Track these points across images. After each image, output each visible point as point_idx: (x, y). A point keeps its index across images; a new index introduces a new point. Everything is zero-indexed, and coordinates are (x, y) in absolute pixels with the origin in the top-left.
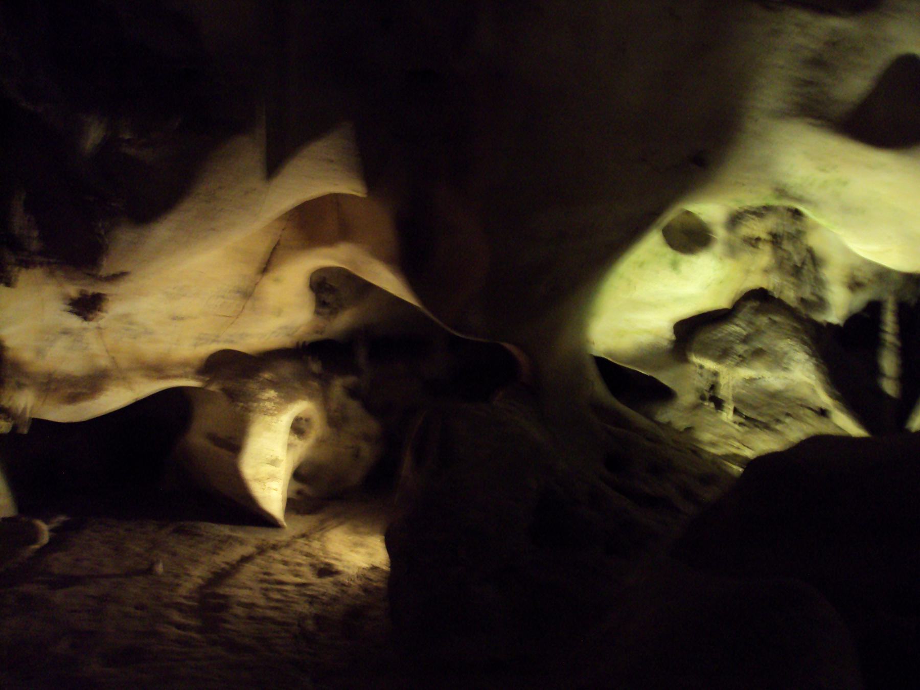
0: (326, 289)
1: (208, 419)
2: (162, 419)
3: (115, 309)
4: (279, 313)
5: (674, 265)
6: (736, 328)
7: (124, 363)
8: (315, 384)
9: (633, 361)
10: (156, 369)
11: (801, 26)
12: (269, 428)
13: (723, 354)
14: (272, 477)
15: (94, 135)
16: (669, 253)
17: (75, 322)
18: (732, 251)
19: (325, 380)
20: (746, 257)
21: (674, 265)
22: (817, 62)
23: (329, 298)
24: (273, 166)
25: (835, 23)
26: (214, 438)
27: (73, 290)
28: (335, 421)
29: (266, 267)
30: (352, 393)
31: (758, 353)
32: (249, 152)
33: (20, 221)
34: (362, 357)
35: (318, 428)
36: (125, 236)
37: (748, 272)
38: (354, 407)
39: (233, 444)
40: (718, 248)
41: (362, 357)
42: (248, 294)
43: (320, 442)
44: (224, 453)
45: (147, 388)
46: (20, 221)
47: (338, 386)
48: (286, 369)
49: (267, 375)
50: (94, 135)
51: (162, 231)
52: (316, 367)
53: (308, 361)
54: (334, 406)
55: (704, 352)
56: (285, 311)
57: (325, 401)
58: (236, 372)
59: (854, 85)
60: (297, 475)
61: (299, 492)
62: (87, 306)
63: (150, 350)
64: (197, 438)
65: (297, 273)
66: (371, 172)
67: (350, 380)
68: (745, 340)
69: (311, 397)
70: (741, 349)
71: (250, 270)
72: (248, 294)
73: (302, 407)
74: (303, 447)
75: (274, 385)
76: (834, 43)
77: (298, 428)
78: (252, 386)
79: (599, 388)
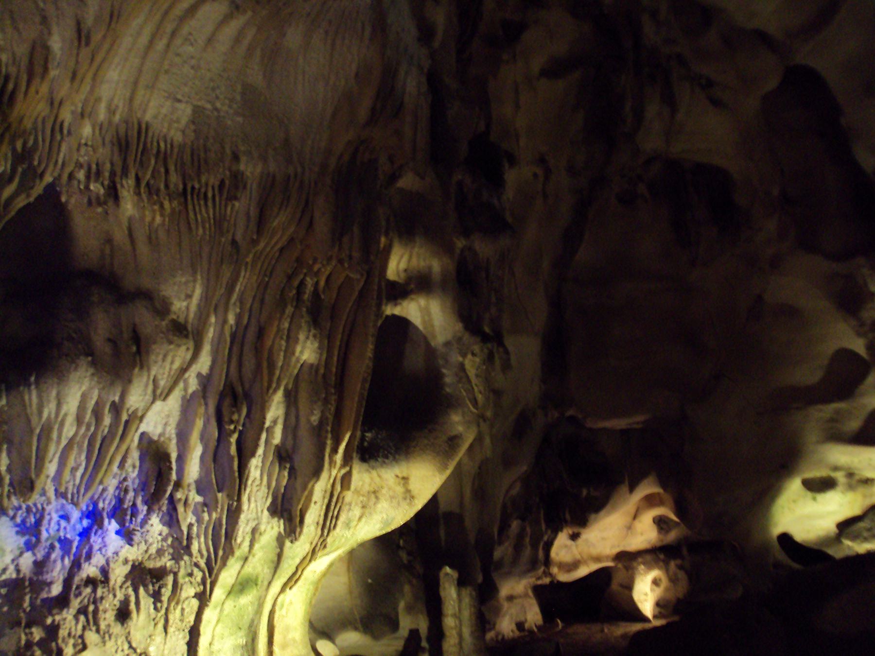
0: (661, 523)
1: (619, 578)
2: (602, 577)
4: (642, 534)
5: (814, 499)
6: (862, 524)
7: (585, 557)
8: (661, 564)
9: (816, 544)
10: (597, 559)
11: (821, 411)
12: (642, 581)
13: (855, 537)
14: (646, 600)
16: (809, 494)
17: (570, 542)
18: (851, 487)
19: (666, 563)
20: (861, 490)
21: (814, 499)
22: (832, 420)
23: (665, 526)
24: (632, 489)
25: (835, 406)
26: (622, 586)
27: (570, 532)
28: (673, 580)
29: (635, 517)
30: (680, 567)
32: (624, 488)
33: (568, 517)
34: (685, 551)
35: (665, 582)
36: (593, 516)
37: (865, 496)
38: (681, 575)
39: (629, 587)
40: (839, 488)
41: (685, 551)
42: (629, 528)
43: (667, 590)
44: (626, 592)
45: (594, 567)
46: (568, 517)
47: (672, 564)
48: (648, 557)
49: (640, 560)
50: (585, 492)
51: (602, 513)
52: (662, 556)
53: (658, 554)
54: (671, 573)
55: (847, 538)
56: (645, 534)
57: (667, 571)
58: (627, 559)
59: (854, 425)
60: (658, 604)
61: (660, 613)
62: (574, 537)
63: (594, 552)
64: (615, 586)
65: (647, 518)
66: (663, 484)
67: (679, 562)
68: (869, 530)
69: (660, 568)
70: (865, 534)
71: (629, 519)
72: (629, 528)
73: (655, 573)
74: (659, 592)
75: (644, 564)
76: (837, 412)
77: (656, 582)
78: (635, 564)
79: (780, 555)
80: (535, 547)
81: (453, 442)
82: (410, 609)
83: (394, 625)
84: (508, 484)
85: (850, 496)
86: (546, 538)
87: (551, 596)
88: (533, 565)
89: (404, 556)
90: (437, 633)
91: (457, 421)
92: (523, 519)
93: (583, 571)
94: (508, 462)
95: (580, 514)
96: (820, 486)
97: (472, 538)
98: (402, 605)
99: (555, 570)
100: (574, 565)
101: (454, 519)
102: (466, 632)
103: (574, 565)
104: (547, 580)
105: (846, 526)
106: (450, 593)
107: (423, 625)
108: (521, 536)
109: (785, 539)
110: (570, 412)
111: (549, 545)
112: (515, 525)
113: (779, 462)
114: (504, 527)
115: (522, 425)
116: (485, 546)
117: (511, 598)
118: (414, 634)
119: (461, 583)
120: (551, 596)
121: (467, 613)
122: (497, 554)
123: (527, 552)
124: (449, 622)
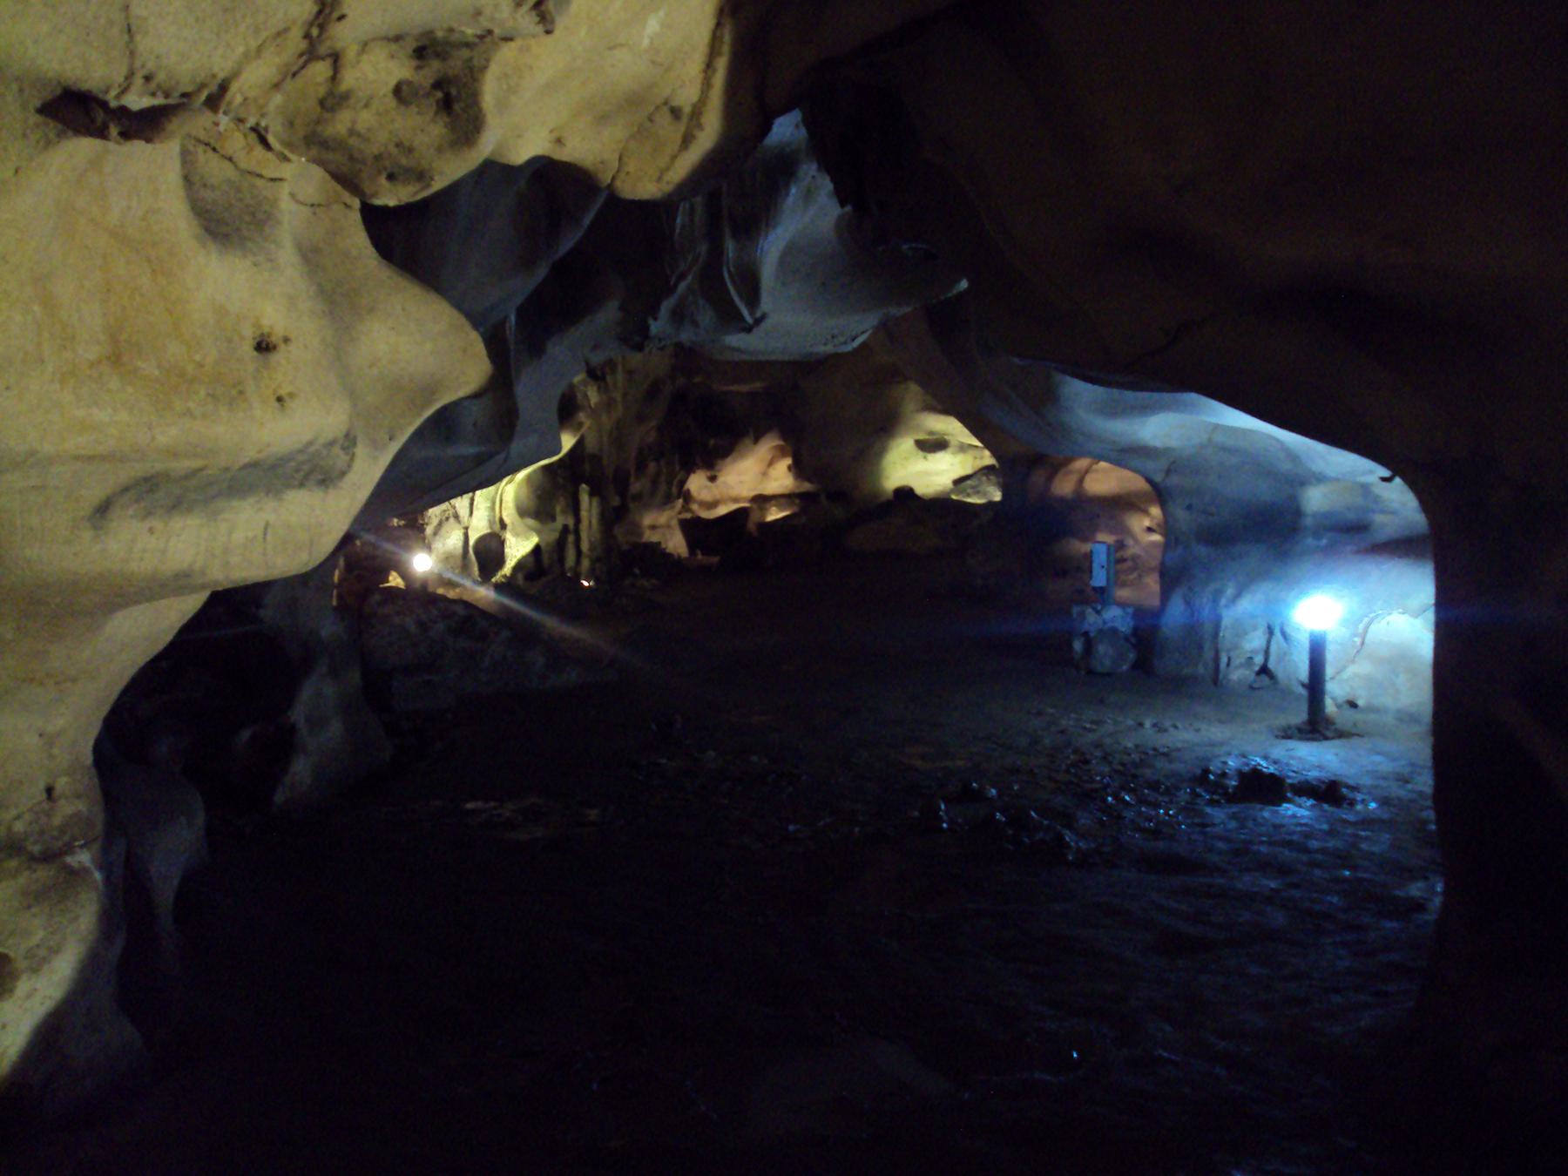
3: (721, 480)
10: (736, 500)
15: (712, 442)
16: (921, 454)
24: (756, 440)
29: (771, 463)
31: (978, 492)
32: (748, 441)
36: (720, 462)
40: (950, 450)
41: (823, 498)
42: (765, 474)
51: (729, 459)
62: (713, 479)
63: (735, 492)
72: (765, 474)
80: (670, 484)
81: (580, 425)
82: (564, 512)
83: (553, 519)
84: (646, 433)
85: (960, 458)
86: (679, 477)
87: (694, 529)
88: (668, 500)
89: (561, 481)
90: (578, 520)
91: (582, 416)
92: (657, 460)
93: (722, 510)
94: (641, 418)
95: (711, 459)
96: (933, 445)
97: (610, 472)
98: (558, 509)
99: (695, 507)
100: (714, 505)
101: (596, 458)
102: (595, 521)
103: (714, 505)
104: (688, 516)
105: (958, 482)
106: (584, 498)
107: (571, 522)
108: (658, 475)
109: (905, 494)
110: (697, 380)
111: (683, 482)
112: (652, 467)
113: (885, 426)
114: (641, 467)
115: (653, 391)
116: (621, 482)
117: (653, 527)
118: (565, 529)
119: (592, 495)
120: (694, 529)
121: (595, 511)
122: (636, 486)
123: (663, 487)
124: (584, 514)
